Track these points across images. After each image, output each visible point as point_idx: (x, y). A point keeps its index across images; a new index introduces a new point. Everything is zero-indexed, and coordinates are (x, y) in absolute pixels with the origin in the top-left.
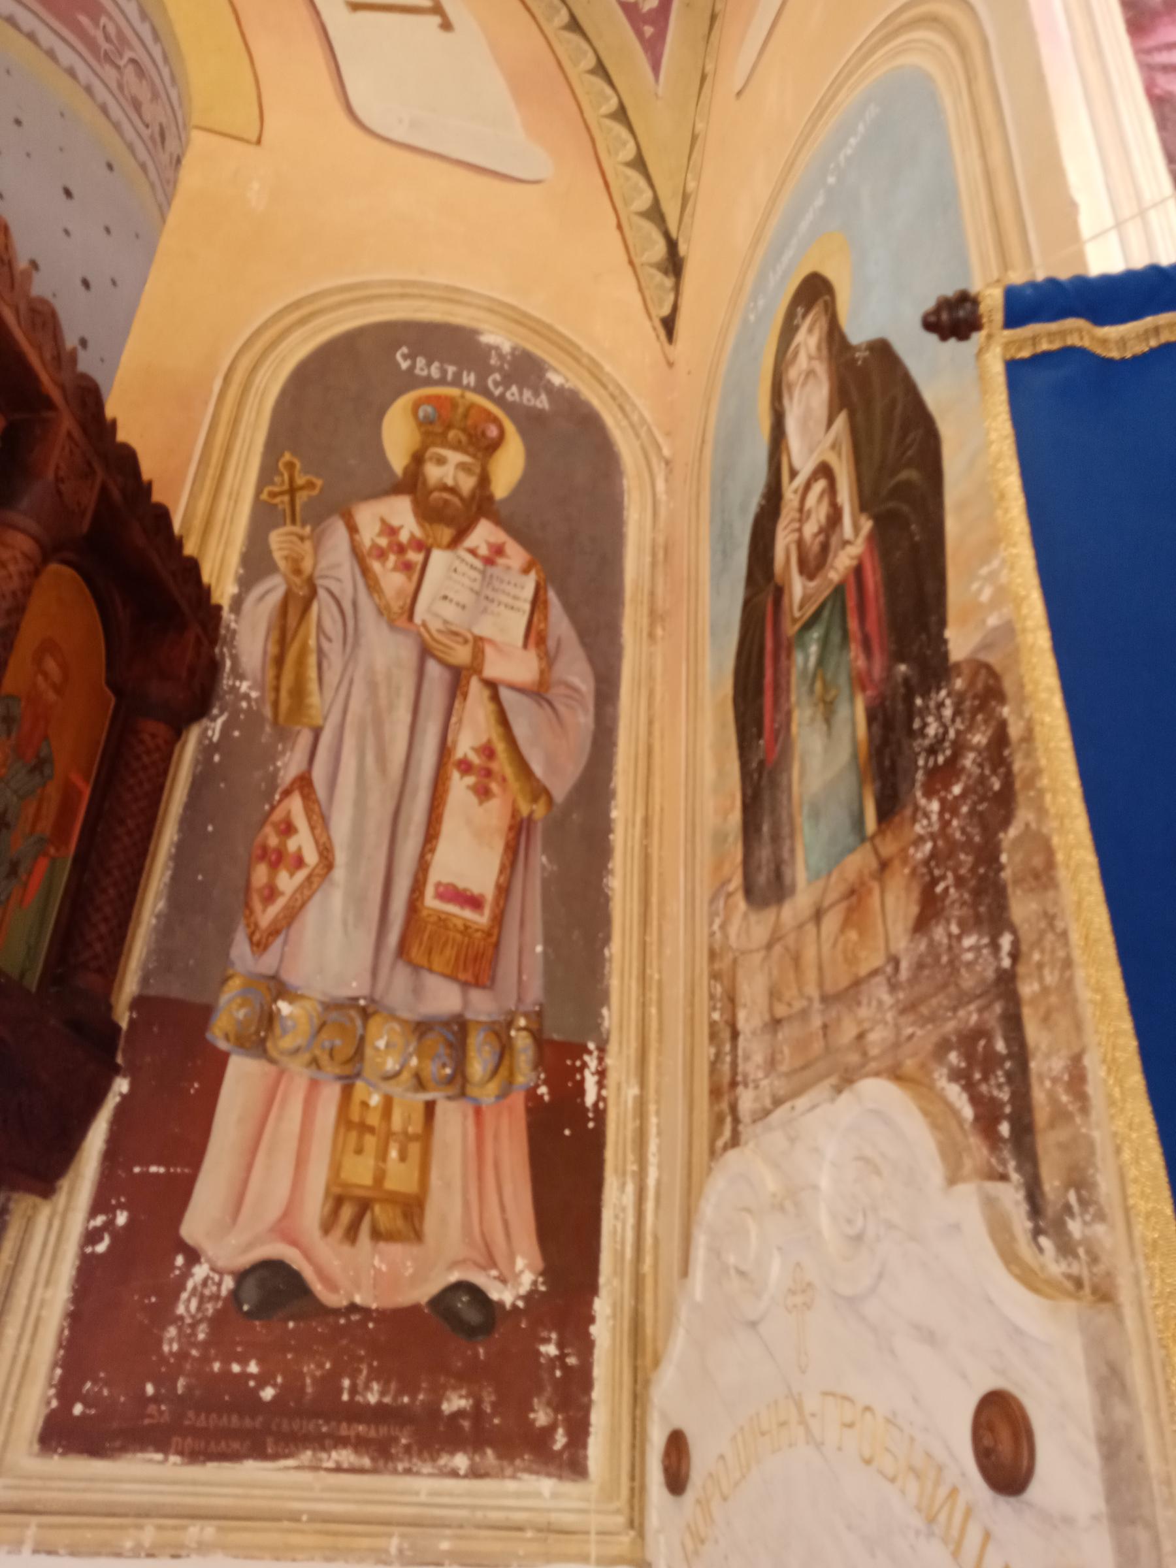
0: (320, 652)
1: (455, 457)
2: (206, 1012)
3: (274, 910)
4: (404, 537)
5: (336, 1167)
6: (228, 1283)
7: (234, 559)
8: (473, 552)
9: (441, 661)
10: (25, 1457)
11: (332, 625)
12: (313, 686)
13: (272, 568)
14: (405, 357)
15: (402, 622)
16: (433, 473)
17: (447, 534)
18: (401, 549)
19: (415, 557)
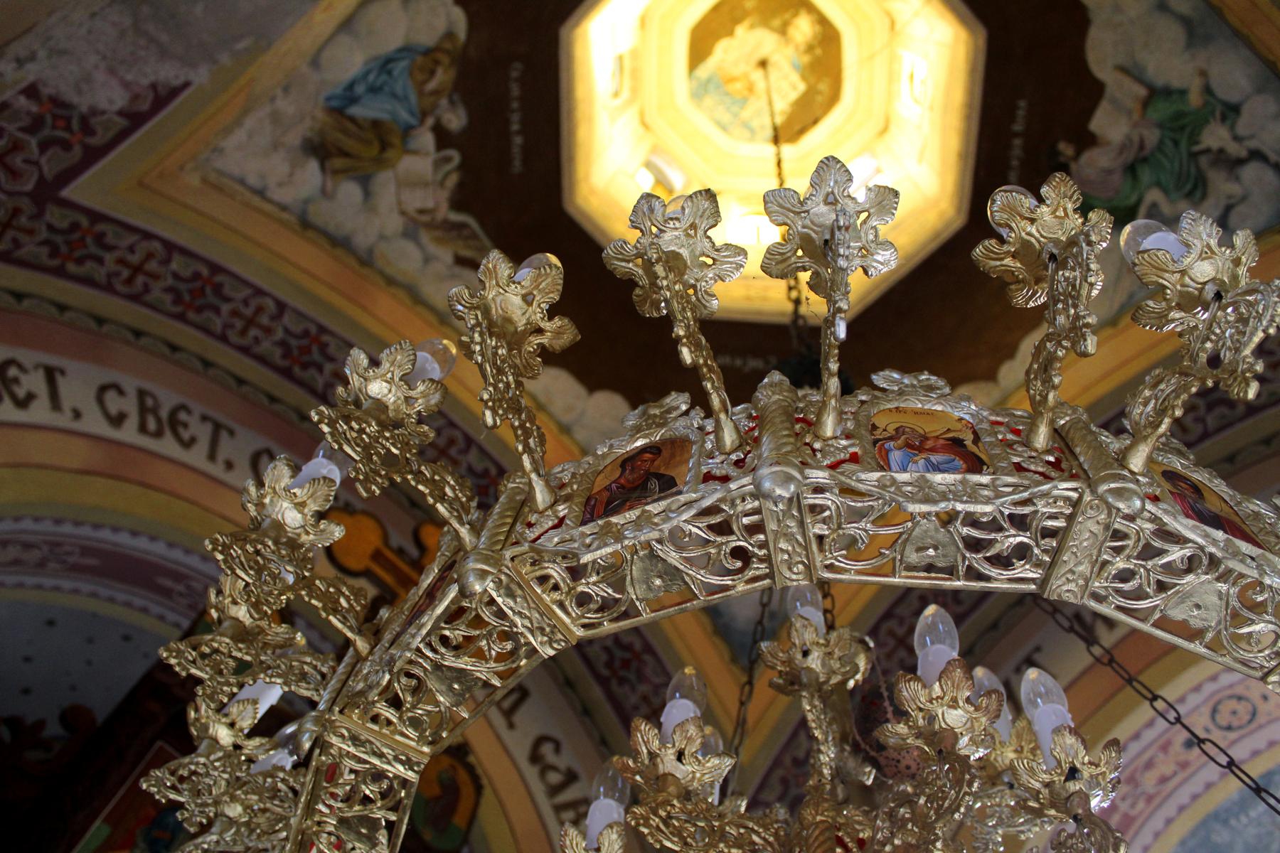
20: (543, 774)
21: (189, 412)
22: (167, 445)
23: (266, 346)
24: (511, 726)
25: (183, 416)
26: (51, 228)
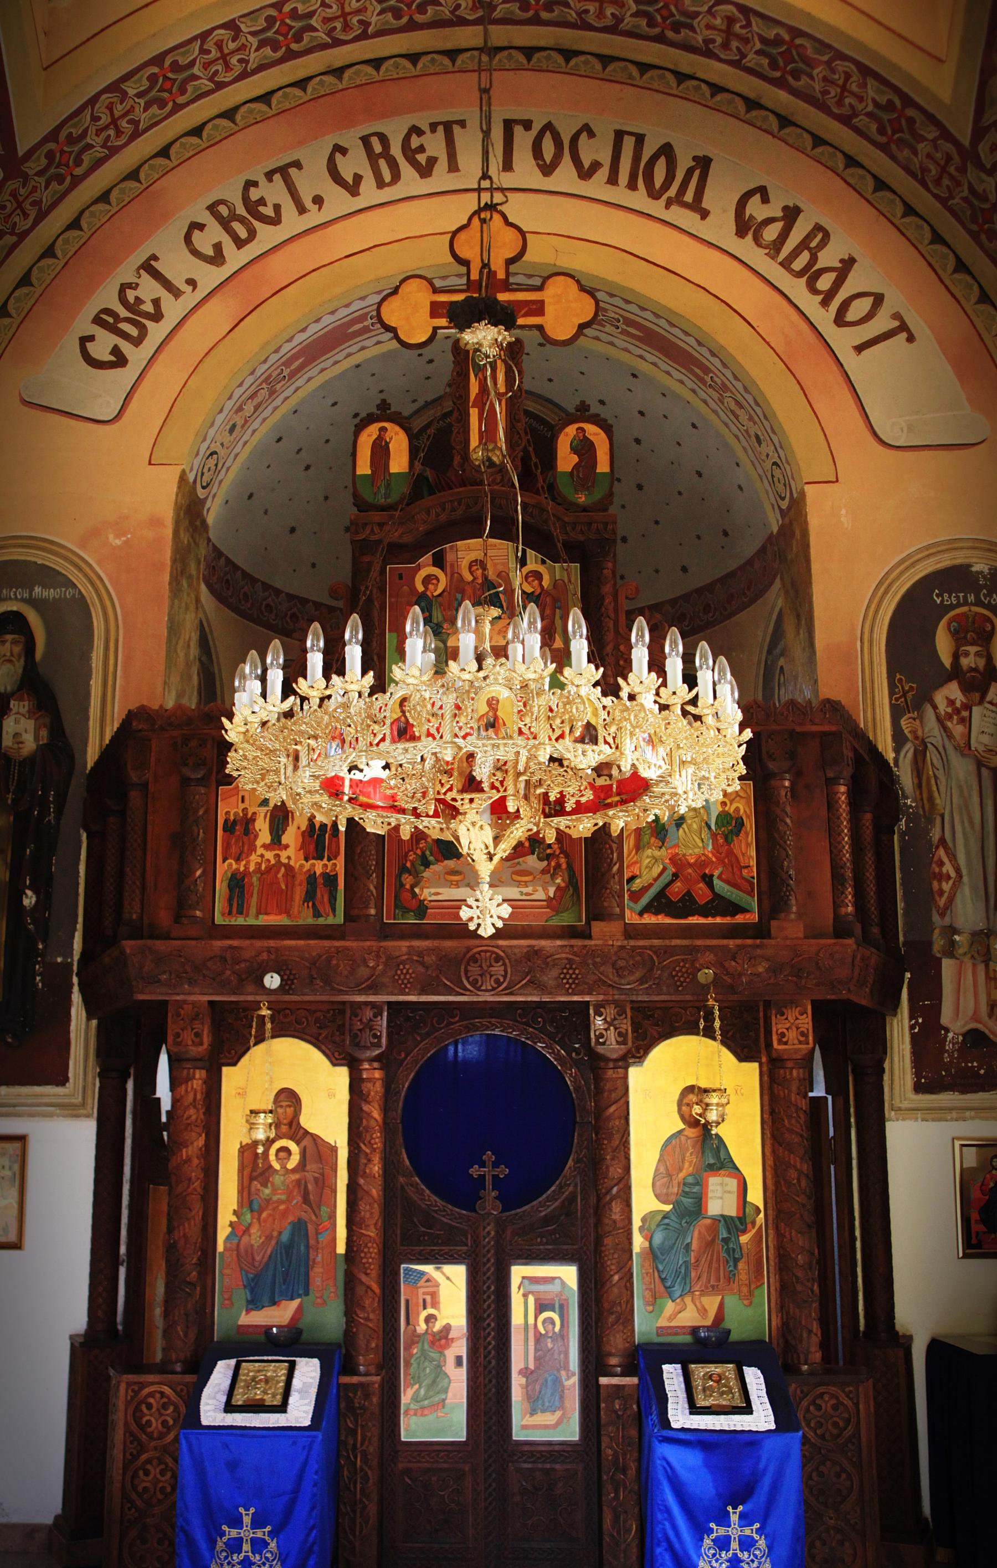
0: (936, 778)
1: (972, 649)
2: (930, 944)
3: (944, 899)
4: (958, 704)
5: (989, 995)
6: (961, 1038)
7: (889, 739)
8: (991, 703)
9: (988, 767)
10: (911, 1095)
11: (937, 763)
12: (936, 794)
13: (907, 740)
14: (938, 596)
15: (966, 752)
16: (965, 662)
17: (977, 696)
18: (957, 711)
19: (965, 714)
20: (757, 240)
21: (255, 184)
22: (267, 236)
23: (254, 59)
24: (704, 214)
25: (254, 194)
26: (39, 174)
